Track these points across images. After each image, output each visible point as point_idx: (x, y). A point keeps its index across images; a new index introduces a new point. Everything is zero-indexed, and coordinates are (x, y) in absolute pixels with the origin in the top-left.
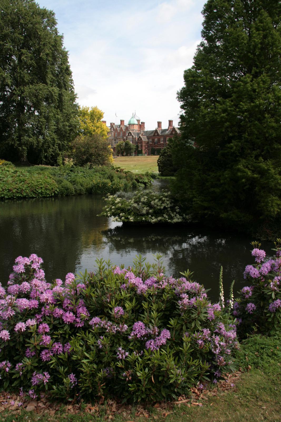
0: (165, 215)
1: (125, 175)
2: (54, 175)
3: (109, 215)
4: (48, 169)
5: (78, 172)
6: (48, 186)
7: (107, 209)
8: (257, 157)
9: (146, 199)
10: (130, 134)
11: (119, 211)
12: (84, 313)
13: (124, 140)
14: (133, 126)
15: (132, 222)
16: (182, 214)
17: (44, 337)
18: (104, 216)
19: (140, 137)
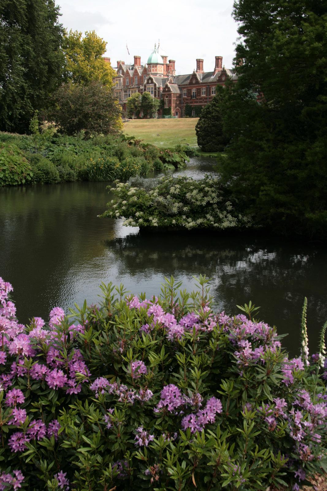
0: (208, 216)
1: (142, 150)
2: (25, 148)
3: (118, 214)
4: (14, 138)
5: (65, 144)
6: (15, 167)
7: (115, 206)
9: (178, 190)
10: (150, 82)
11: (134, 209)
12: (81, 371)
13: (140, 91)
14: (156, 66)
15: (156, 227)
16: (236, 214)
17: (15, 412)
18: (109, 216)
19: (167, 86)
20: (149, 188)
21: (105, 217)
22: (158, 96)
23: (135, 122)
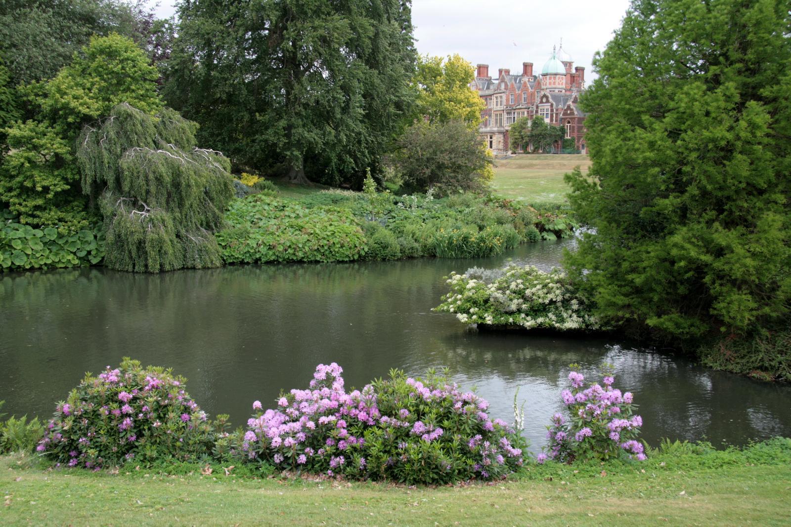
0: (550, 315)
3: (452, 310)
8: (709, 223)
10: (544, 100)
12: (375, 413)
14: (555, 78)
17: (342, 430)
19: (569, 107)
20: (489, 281)
21: (440, 312)
22: (556, 121)
23: (521, 158)
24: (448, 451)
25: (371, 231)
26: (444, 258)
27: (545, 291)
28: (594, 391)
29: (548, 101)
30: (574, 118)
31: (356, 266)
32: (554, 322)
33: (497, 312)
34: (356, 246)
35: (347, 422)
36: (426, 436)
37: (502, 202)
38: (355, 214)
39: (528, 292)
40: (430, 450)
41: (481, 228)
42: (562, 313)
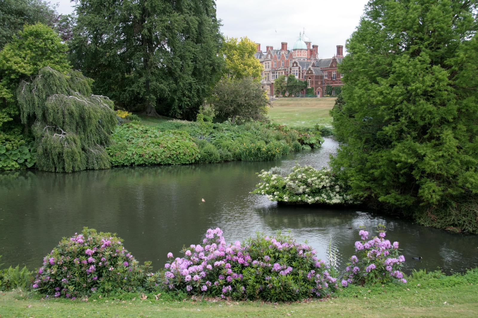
0: (323, 195)
3: (263, 193)
10: (295, 65)
12: (249, 259)
14: (301, 52)
17: (229, 269)
19: (310, 69)
20: (285, 175)
22: (302, 77)
24: (296, 281)
25: (202, 145)
26: (246, 161)
27: (319, 180)
28: (376, 242)
29: (297, 66)
30: (313, 76)
31: (193, 167)
32: (326, 200)
33: (291, 194)
34: (193, 155)
35: (231, 264)
36: (282, 272)
37: (278, 127)
38: (190, 135)
39: (309, 180)
40: (286, 280)
41: (267, 143)
42: (330, 194)
